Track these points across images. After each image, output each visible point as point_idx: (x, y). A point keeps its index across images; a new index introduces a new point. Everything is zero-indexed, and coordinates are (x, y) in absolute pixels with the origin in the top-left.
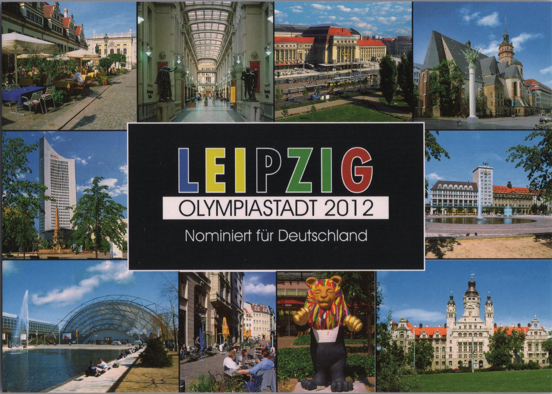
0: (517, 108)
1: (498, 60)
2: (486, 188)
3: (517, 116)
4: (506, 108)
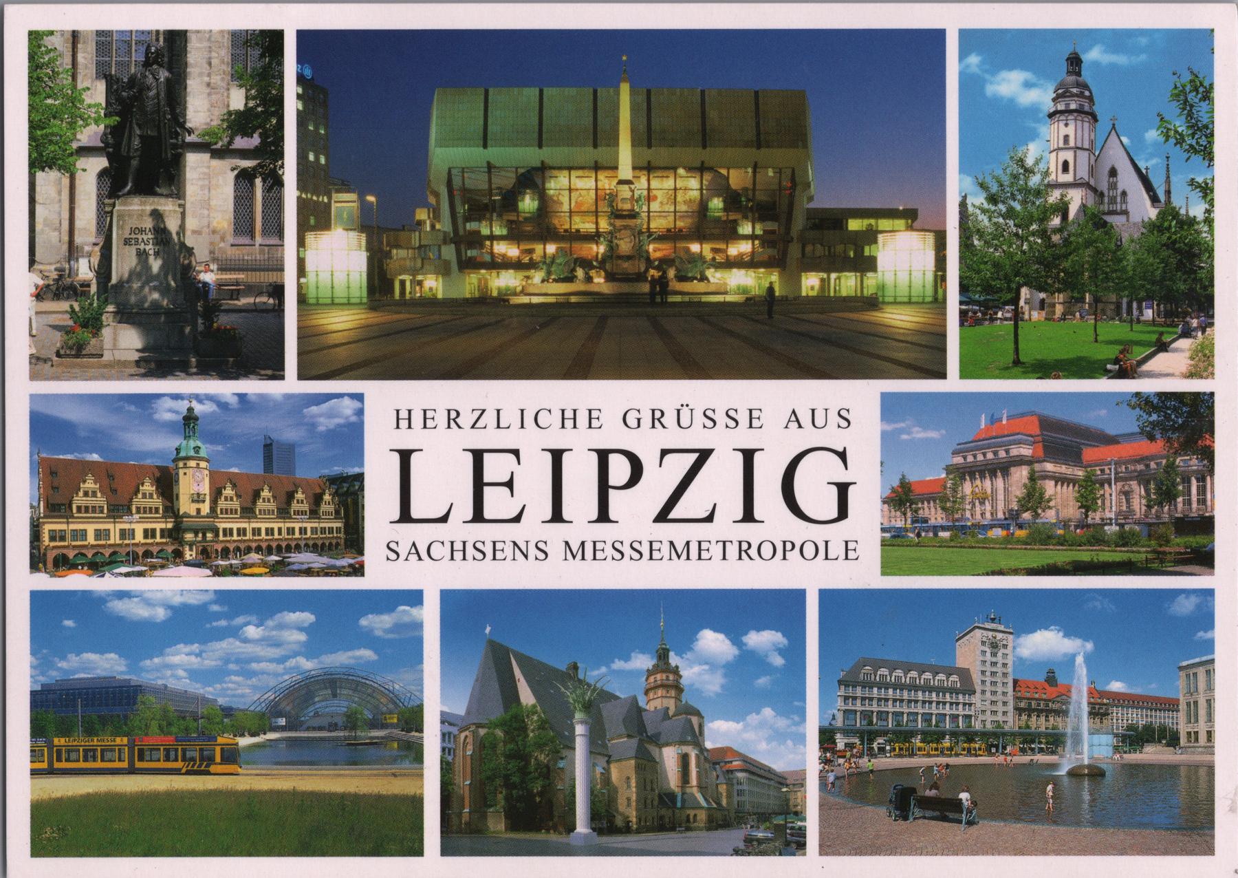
0: (688, 812)
1: (641, 704)
3: (688, 829)
4: (663, 812)
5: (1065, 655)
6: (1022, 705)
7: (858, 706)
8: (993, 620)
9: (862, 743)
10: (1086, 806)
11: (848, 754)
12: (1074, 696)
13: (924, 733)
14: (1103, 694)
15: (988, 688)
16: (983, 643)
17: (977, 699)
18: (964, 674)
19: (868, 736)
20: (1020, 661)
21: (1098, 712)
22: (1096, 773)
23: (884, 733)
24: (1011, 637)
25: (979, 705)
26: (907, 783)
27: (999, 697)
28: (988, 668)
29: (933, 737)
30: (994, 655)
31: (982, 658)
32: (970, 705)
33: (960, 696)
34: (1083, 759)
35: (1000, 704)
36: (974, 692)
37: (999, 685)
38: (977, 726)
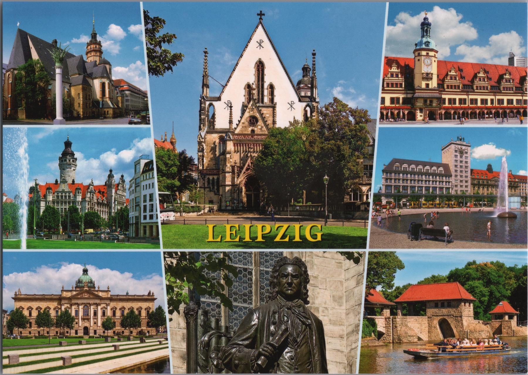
2: (461, 171)
5: (497, 157)
6: (476, 182)
7: (393, 183)
8: (461, 140)
9: (395, 201)
10: (507, 233)
11: (388, 207)
12: (501, 178)
13: (426, 196)
14: (516, 177)
15: (459, 173)
16: (456, 151)
17: (452, 179)
18: (446, 167)
19: (398, 198)
20: (474, 159)
21: (513, 186)
22: (512, 216)
23: (405, 196)
24: (469, 148)
25: (453, 182)
26: (418, 222)
27: (464, 179)
28: (459, 164)
29: (431, 198)
30: (461, 157)
31: (455, 159)
32: (449, 182)
33: (444, 178)
34: (505, 209)
35: (464, 182)
36: (451, 176)
37: (464, 172)
38: (453, 192)
